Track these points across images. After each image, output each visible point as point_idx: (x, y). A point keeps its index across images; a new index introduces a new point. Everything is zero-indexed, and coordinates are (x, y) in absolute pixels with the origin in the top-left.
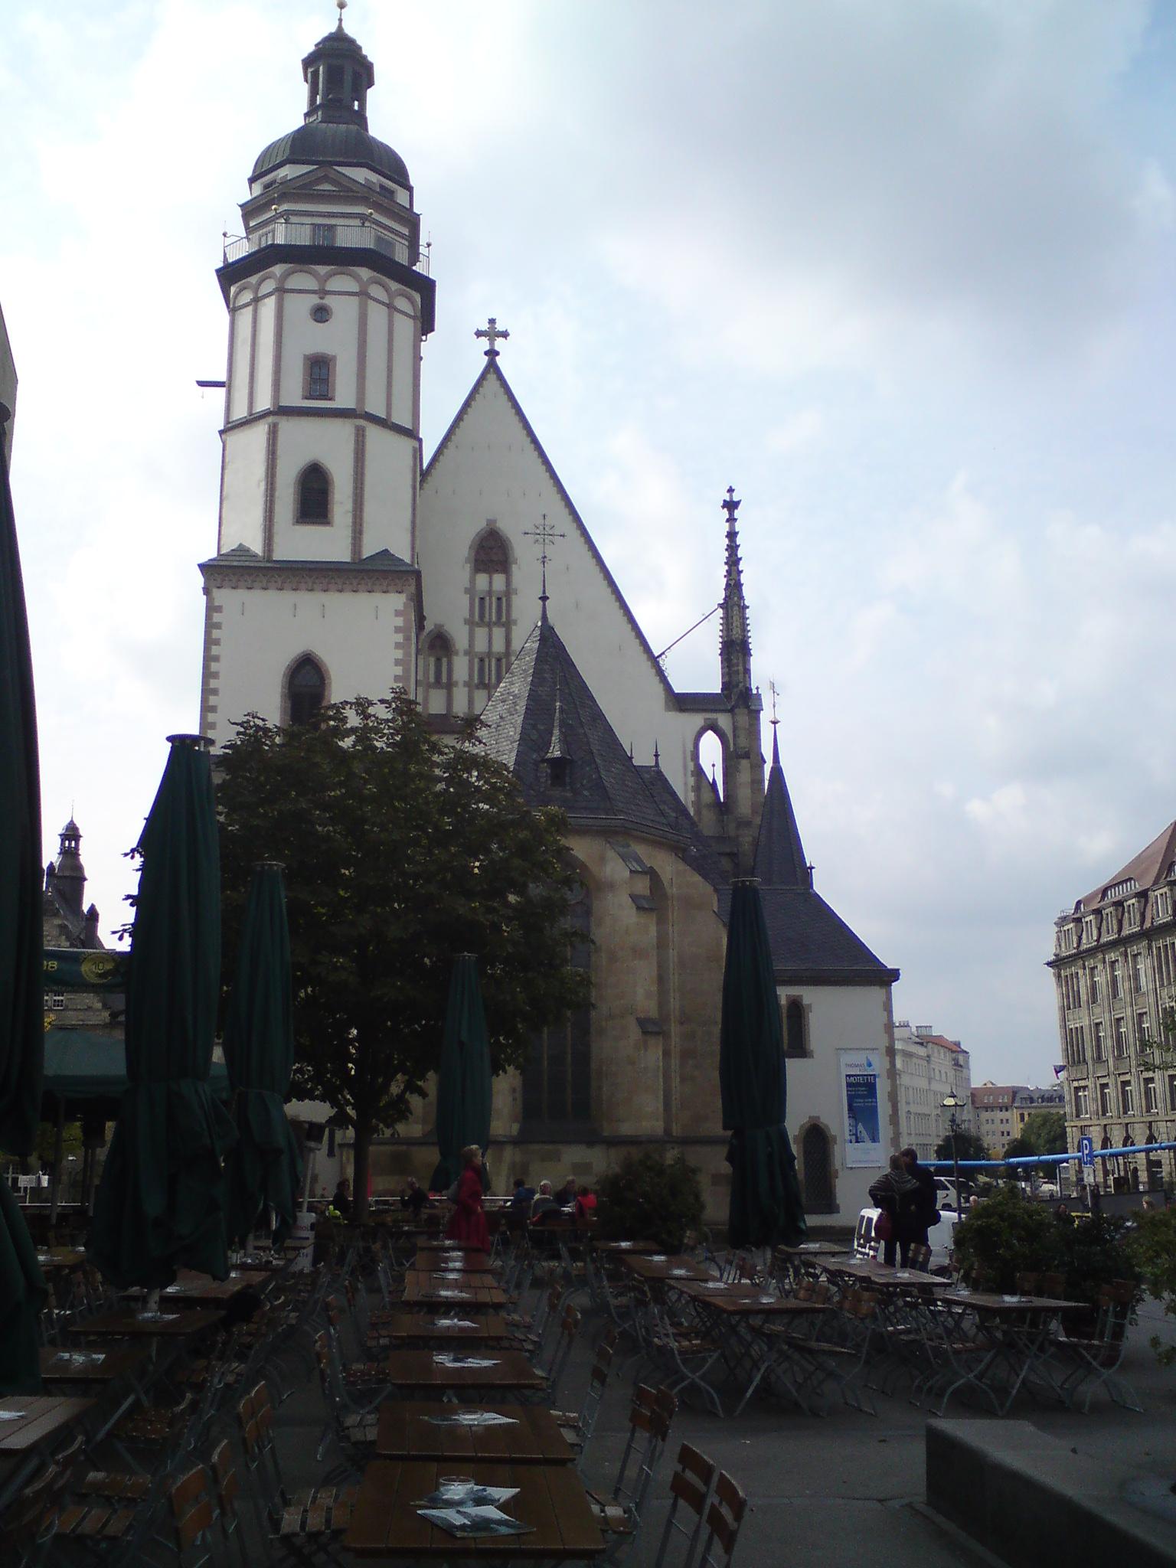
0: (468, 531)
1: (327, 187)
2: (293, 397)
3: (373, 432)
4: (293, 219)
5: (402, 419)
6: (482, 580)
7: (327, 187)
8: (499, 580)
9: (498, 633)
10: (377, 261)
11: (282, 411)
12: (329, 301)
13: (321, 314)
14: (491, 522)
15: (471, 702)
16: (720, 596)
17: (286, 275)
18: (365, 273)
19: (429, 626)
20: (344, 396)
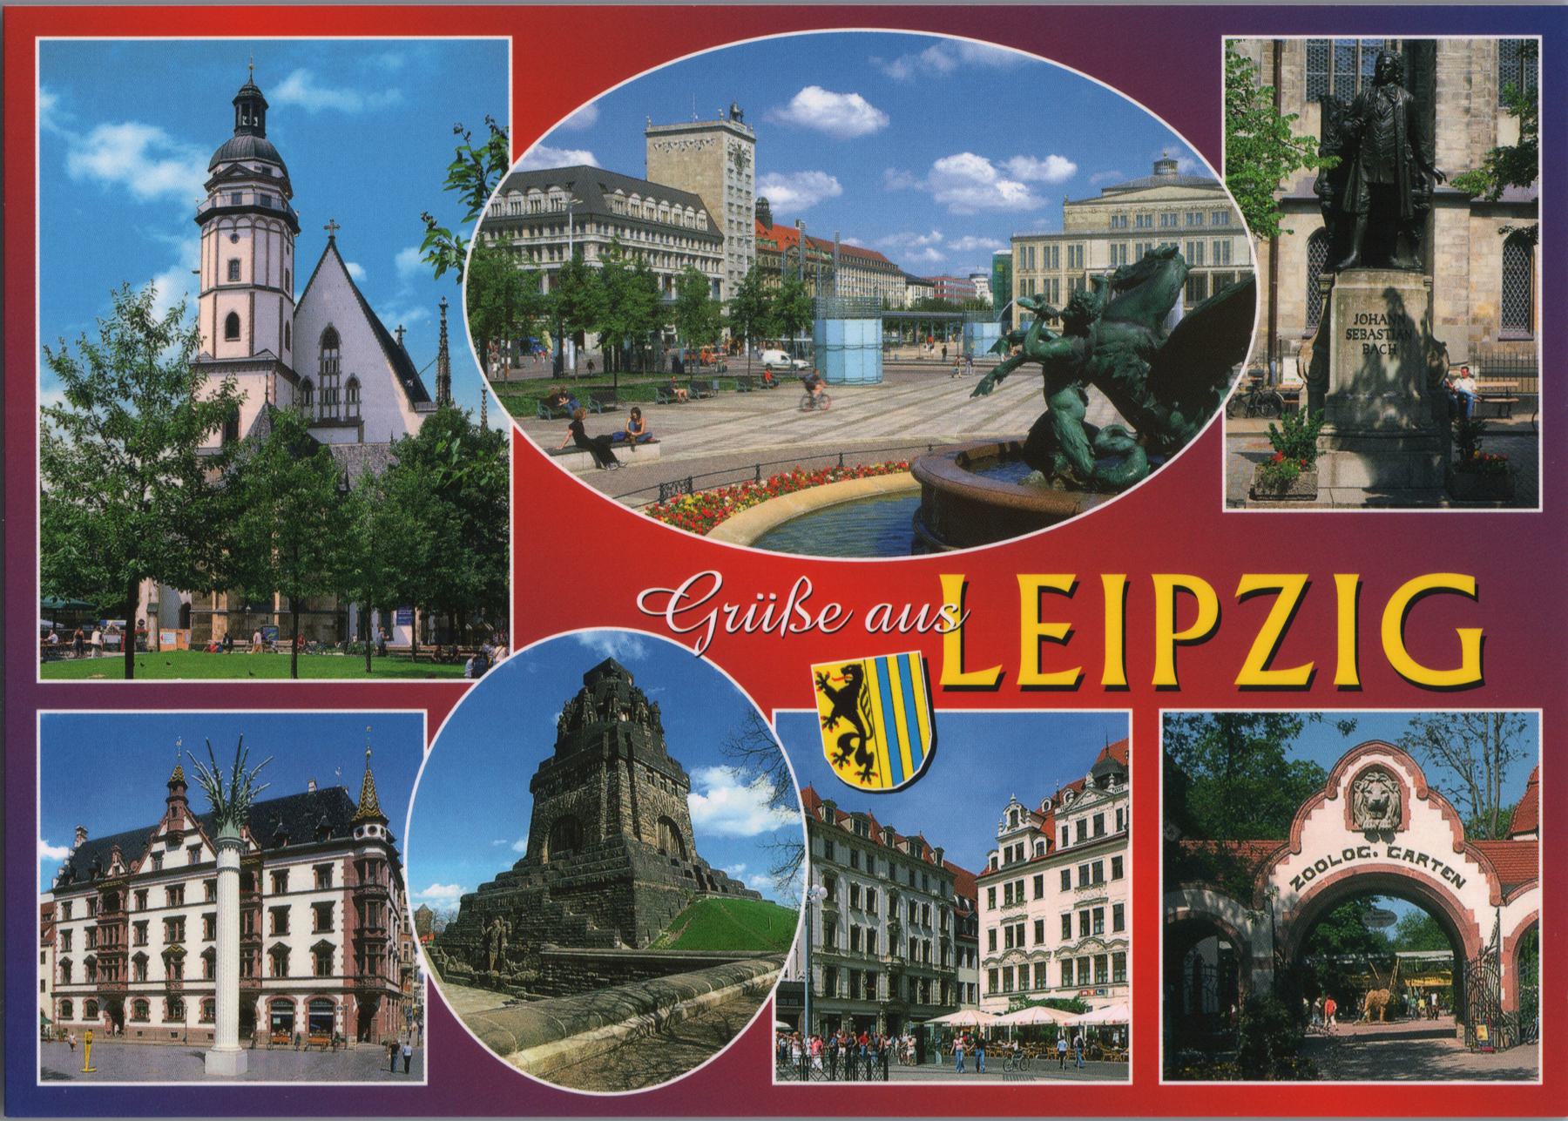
0: (319, 330)
1: (237, 174)
2: (224, 281)
3: (259, 295)
4: (224, 192)
5: (275, 283)
6: (327, 352)
7: (237, 174)
8: (334, 352)
9: (334, 378)
10: (262, 210)
11: (219, 289)
12: (239, 232)
13: (234, 238)
14: (330, 324)
15: (322, 411)
16: (438, 352)
17: (219, 222)
18: (253, 216)
19: (302, 378)
20: (245, 278)
